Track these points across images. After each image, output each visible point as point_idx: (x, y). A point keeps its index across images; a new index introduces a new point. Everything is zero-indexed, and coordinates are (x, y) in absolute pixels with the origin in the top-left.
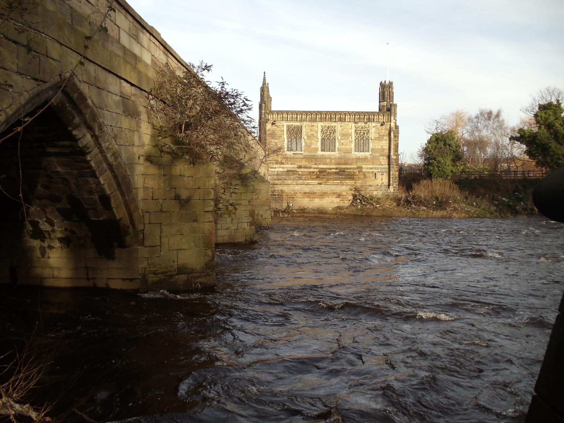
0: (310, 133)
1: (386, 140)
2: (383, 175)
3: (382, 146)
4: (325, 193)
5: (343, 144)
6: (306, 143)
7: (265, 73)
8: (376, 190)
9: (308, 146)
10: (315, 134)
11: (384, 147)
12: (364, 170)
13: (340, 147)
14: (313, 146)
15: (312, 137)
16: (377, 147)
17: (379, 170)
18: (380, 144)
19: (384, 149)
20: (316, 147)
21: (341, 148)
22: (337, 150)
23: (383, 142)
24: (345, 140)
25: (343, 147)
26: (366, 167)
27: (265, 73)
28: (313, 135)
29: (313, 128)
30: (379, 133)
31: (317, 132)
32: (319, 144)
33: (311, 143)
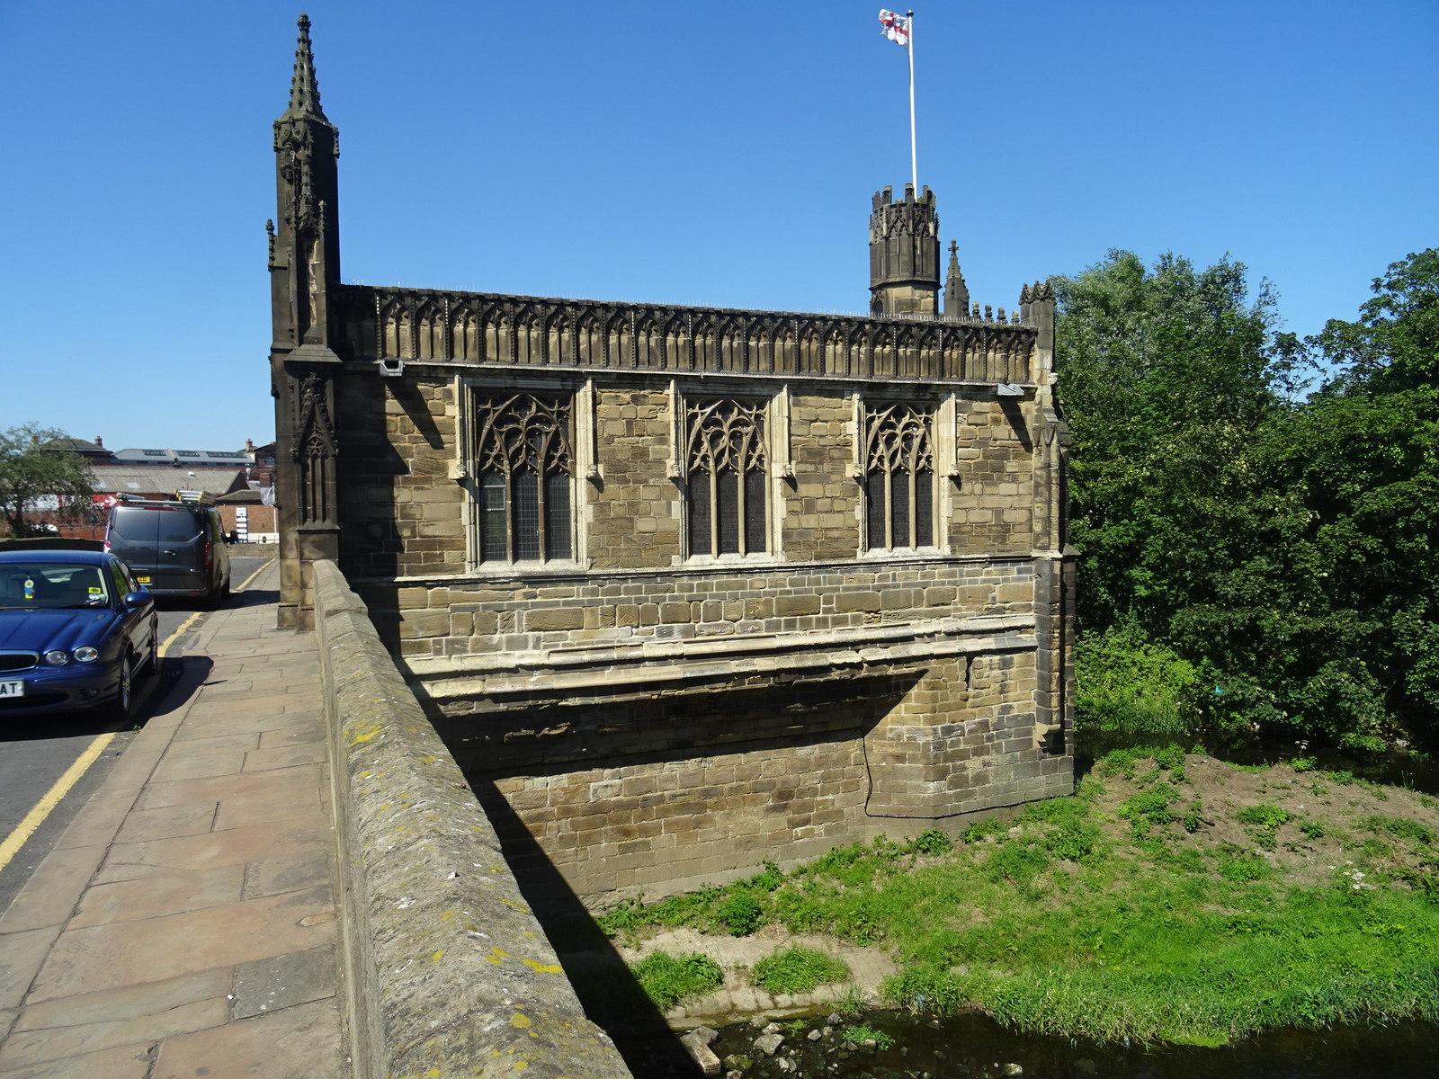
0: (623, 446)
1: (1014, 478)
2: (1006, 665)
3: (998, 512)
4: (707, 793)
5: (809, 506)
6: (601, 508)
7: (305, 24)
8: (979, 752)
9: (612, 526)
10: (654, 450)
11: (1008, 517)
12: (916, 649)
13: (794, 524)
14: (644, 525)
15: (639, 467)
16: (975, 517)
17: (989, 643)
18: (990, 502)
19: (1005, 529)
20: (665, 525)
21: (805, 532)
22: (775, 538)
23: (1005, 488)
24: (824, 479)
25: (810, 521)
26: (928, 633)
27: (305, 24)
28: (641, 454)
29: (642, 411)
30: (982, 443)
31: (662, 439)
32: (678, 508)
33: (633, 506)
